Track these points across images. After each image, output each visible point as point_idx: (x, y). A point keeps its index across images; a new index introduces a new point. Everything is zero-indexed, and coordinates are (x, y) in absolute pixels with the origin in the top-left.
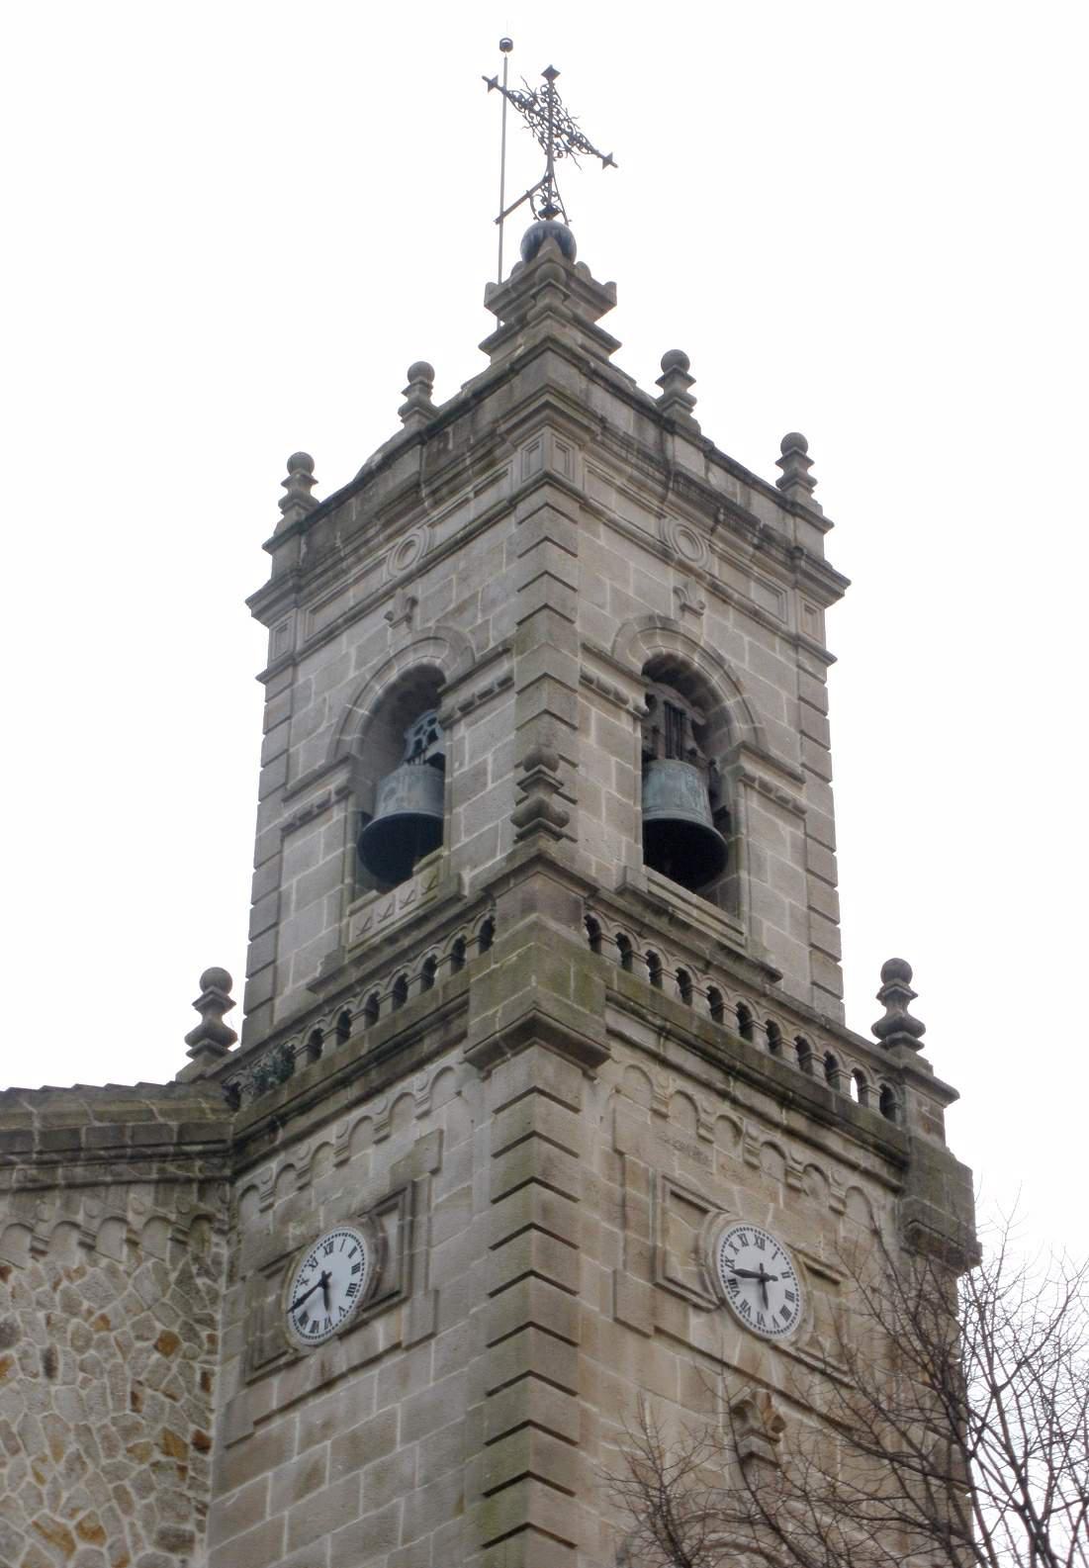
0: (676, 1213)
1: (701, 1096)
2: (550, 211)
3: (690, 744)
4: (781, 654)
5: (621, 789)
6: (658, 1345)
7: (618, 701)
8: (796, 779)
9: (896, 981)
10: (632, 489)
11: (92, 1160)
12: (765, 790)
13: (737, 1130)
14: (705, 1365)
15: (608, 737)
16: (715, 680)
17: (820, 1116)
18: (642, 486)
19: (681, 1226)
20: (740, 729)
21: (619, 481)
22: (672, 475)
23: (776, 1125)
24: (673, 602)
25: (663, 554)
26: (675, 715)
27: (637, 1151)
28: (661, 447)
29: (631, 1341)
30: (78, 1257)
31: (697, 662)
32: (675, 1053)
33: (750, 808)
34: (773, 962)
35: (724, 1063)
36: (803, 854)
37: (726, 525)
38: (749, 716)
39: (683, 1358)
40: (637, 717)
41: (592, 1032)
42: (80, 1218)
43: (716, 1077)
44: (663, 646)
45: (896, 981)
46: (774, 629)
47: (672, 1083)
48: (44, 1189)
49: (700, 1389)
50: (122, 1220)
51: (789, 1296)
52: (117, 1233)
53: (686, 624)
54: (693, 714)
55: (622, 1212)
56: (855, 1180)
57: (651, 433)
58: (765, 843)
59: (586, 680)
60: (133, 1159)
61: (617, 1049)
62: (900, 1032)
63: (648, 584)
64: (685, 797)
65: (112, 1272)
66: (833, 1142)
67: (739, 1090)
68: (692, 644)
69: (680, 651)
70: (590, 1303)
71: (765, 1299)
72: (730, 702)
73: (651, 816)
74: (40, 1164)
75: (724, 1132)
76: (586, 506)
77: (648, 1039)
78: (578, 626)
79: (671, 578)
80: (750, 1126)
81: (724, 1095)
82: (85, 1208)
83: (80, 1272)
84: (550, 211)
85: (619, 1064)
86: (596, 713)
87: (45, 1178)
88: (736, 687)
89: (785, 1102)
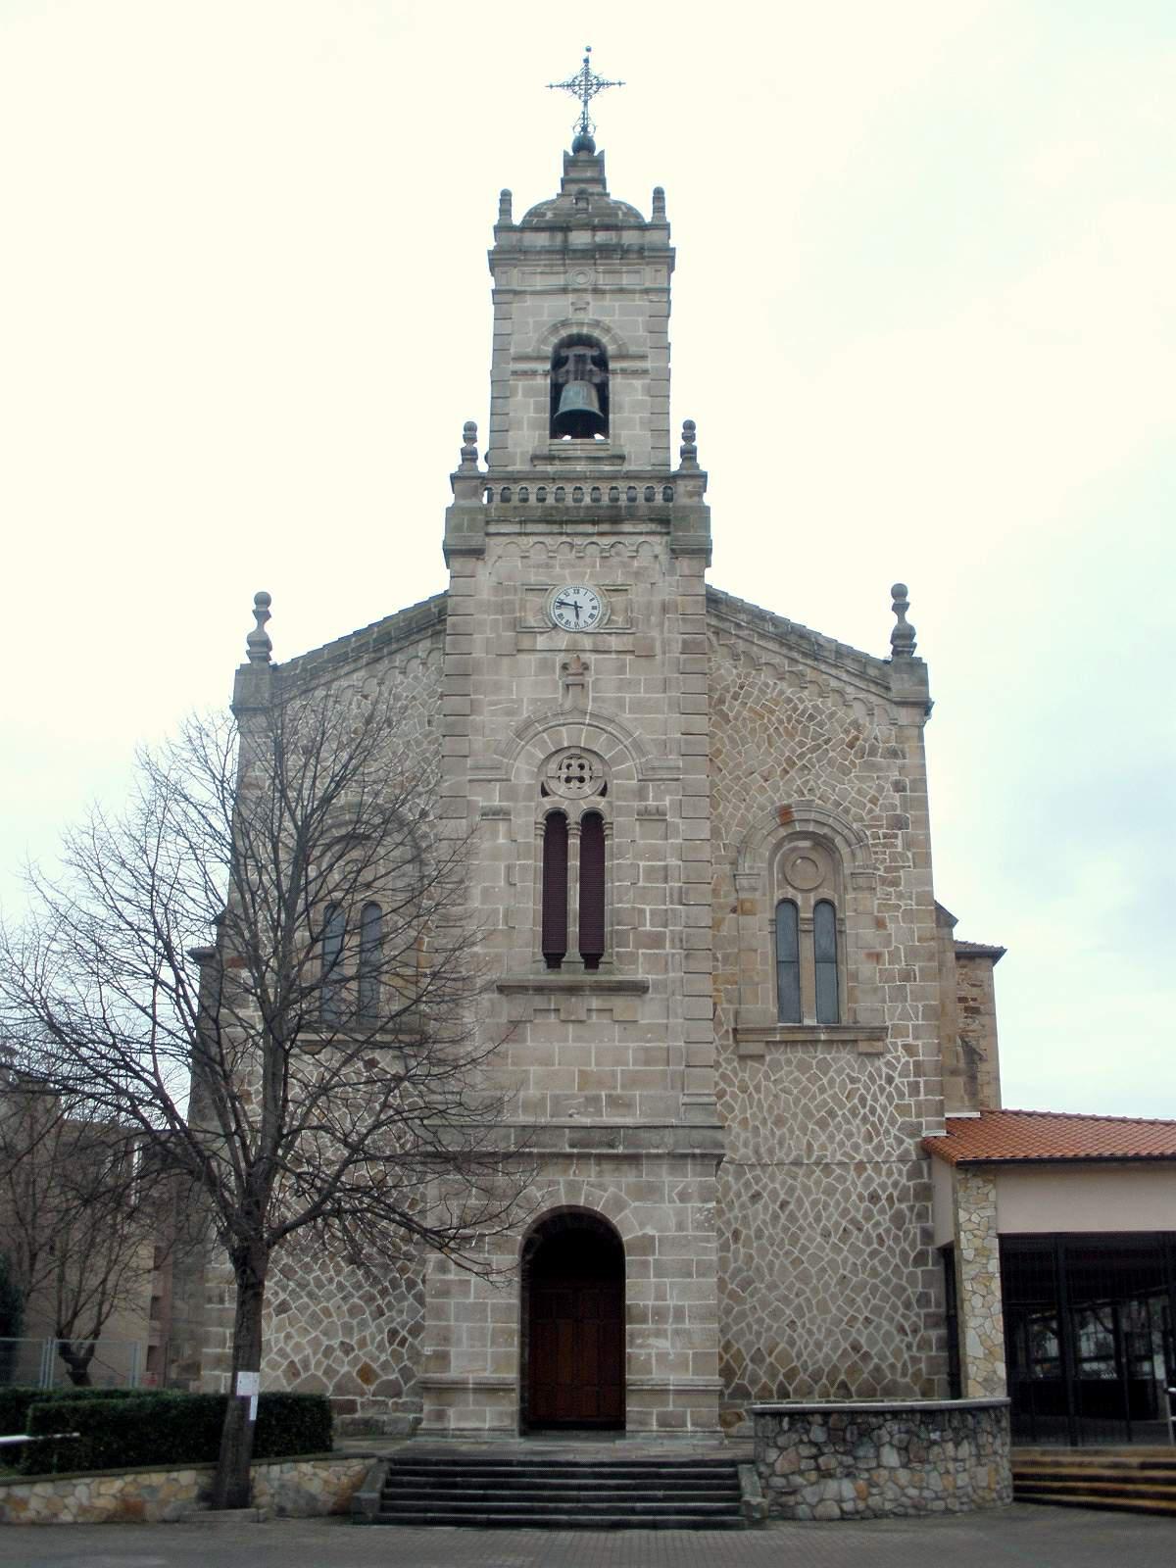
0: (530, 596)
1: (548, 540)
2: (584, 129)
3: (590, 366)
4: (639, 301)
5: (537, 410)
6: (520, 656)
7: (534, 373)
8: (643, 357)
9: (689, 426)
10: (547, 270)
11: (398, 641)
12: (624, 371)
13: (572, 545)
14: (548, 655)
15: (529, 392)
16: (596, 333)
17: (616, 520)
18: (552, 266)
19: (534, 599)
20: (611, 349)
21: (539, 270)
22: (565, 251)
23: (593, 534)
24: (571, 309)
25: (564, 290)
26: (580, 359)
27: (510, 578)
28: (566, 240)
29: (506, 661)
30: (400, 678)
31: (585, 331)
32: (530, 528)
33: (616, 384)
34: (626, 451)
35: (557, 519)
36: (648, 391)
37: (601, 258)
38: (614, 340)
39: (532, 657)
40: (546, 374)
41: (477, 540)
42: (397, 664)
43: (555, 528)
44: (564, 333)
45: (689, 426)
46: (633, 292)
47: (532, 540)
48: (377, 660)
49: (545, 667)
50: (417, 657)
51: (594, 608)
52: (415, 663)
53: (581, 316)
54: (590, 352)
55: (500, 609)
56: (642, 539)
57: (559, 236)
58: (626, 394)
59: (514, 373)
60: (418, 632)
61: (492, 541)
62: (689, 454)
63: (560, 307)
64: (578, 397)
65: (416, 678)
66: (627, 527)
67: (569, 529)
68: (582, 324)
69: (575, 330)
70: (479, 654)
71: (577, 616)
72: (605, 340)
73: (563, 408)
74: (374, 651)
75: (566, 548)
76: (516, 293)
77: (516, 528)
78: (512, 351)
79: (571, 298)
80: (578, 541)
81: (561, 534)
82: (399, 659)
83: (402, 683)
84: (584, 129)
85: (495, 546)
86: (521, 384)
87: (379, 655)
88: (608, 330)
89: (594, 523)
